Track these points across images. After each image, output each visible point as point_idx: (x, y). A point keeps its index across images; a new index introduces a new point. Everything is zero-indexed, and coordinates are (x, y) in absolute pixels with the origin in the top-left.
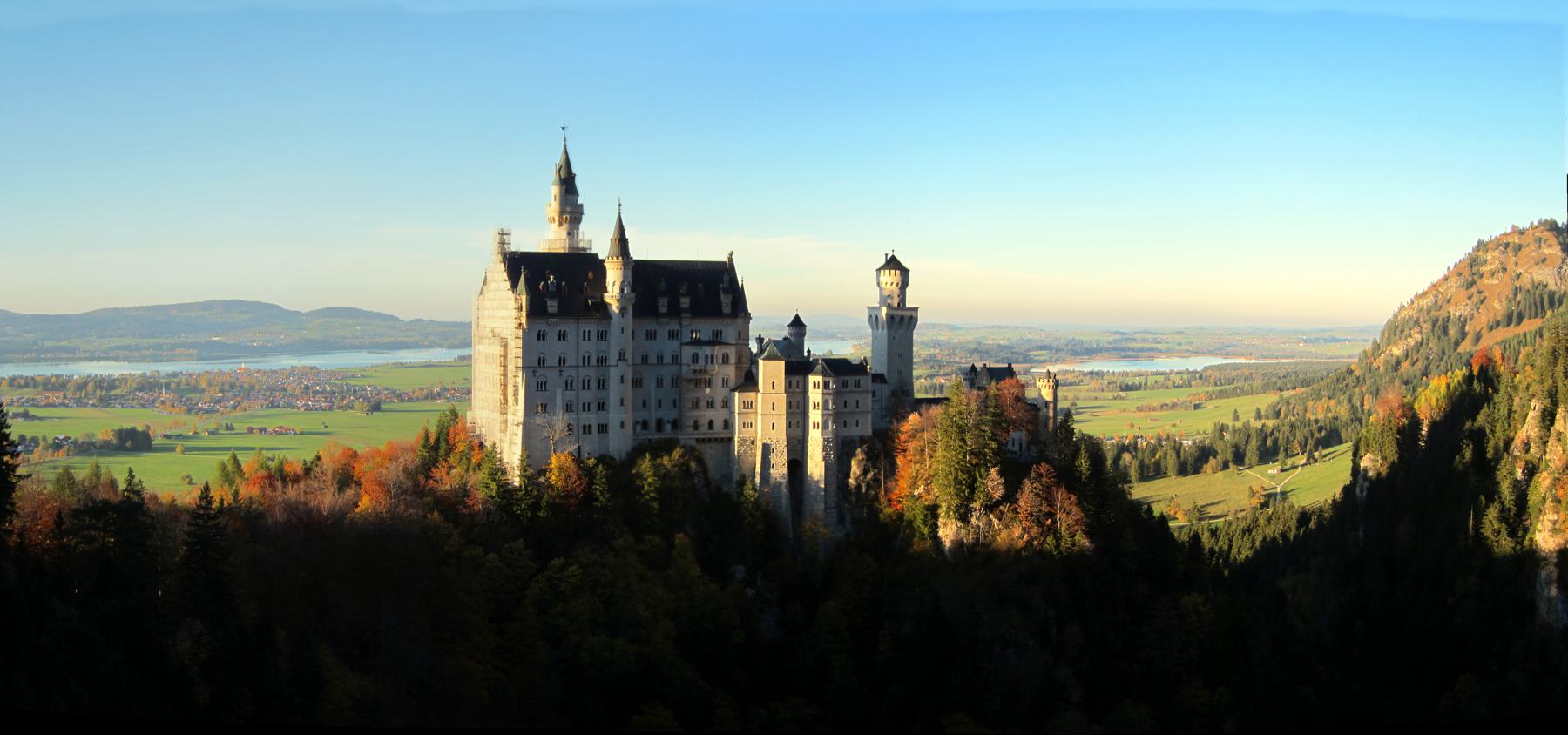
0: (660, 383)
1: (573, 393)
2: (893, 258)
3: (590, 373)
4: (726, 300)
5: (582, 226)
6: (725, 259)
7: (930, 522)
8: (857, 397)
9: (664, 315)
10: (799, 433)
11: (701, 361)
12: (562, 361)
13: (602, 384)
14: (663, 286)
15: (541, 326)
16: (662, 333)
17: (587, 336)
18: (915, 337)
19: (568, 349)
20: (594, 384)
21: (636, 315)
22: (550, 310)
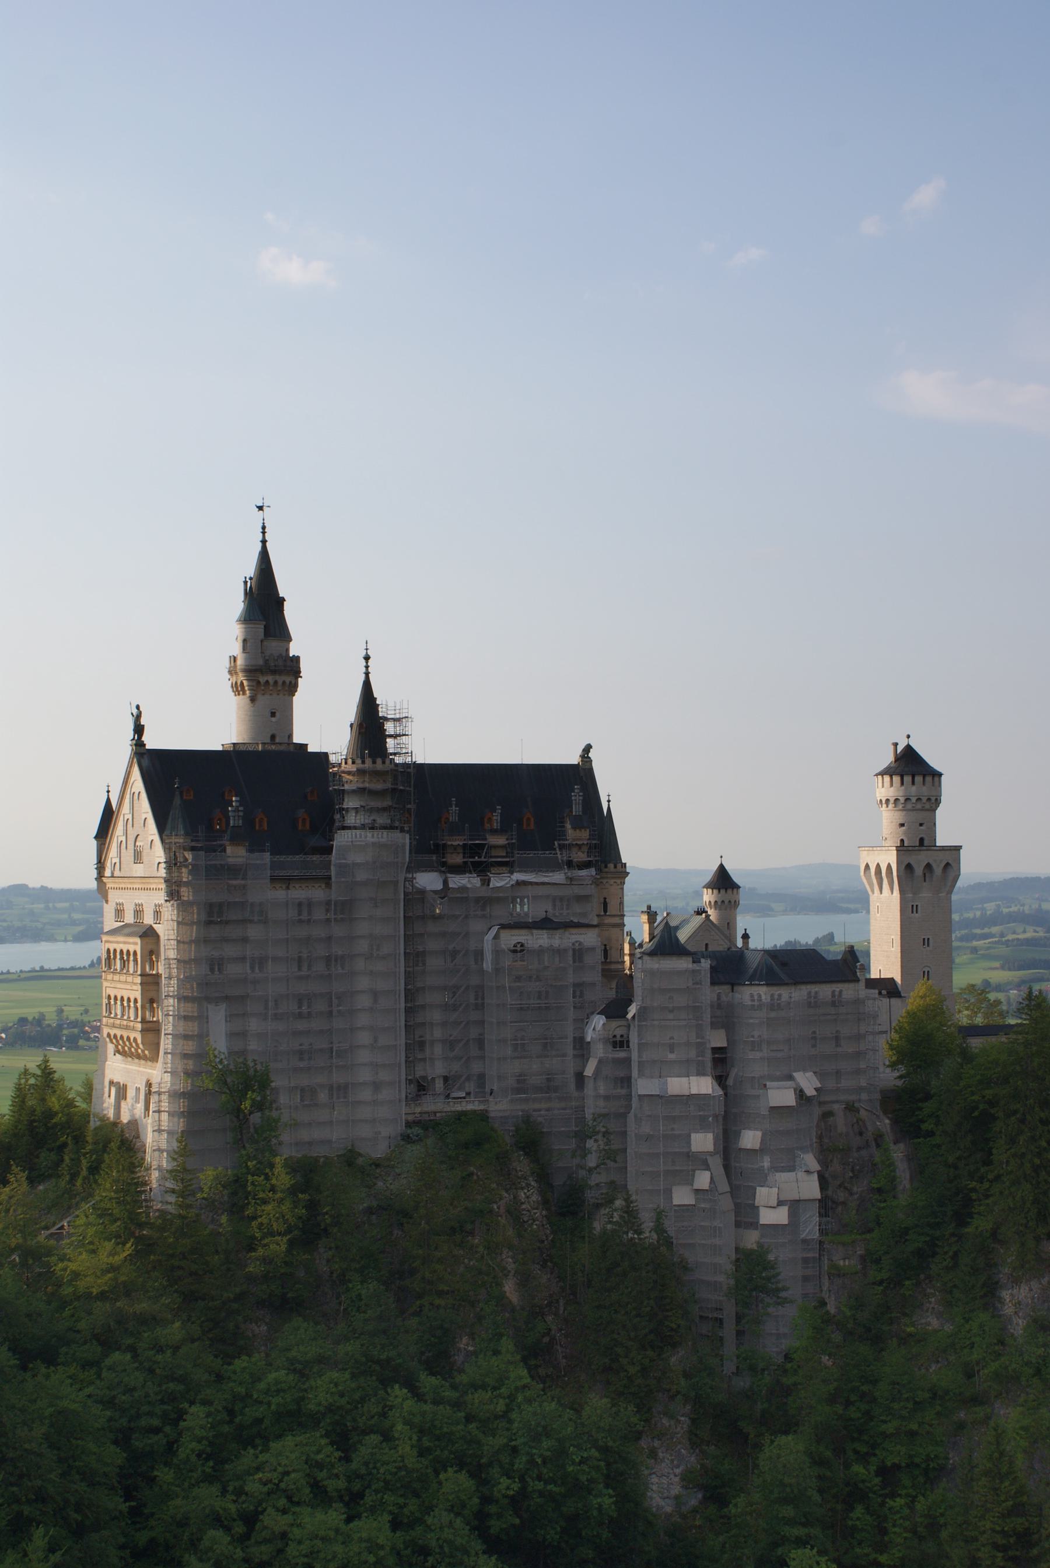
5: (297, 699)
6: (574, 759)
14: (453, 812)
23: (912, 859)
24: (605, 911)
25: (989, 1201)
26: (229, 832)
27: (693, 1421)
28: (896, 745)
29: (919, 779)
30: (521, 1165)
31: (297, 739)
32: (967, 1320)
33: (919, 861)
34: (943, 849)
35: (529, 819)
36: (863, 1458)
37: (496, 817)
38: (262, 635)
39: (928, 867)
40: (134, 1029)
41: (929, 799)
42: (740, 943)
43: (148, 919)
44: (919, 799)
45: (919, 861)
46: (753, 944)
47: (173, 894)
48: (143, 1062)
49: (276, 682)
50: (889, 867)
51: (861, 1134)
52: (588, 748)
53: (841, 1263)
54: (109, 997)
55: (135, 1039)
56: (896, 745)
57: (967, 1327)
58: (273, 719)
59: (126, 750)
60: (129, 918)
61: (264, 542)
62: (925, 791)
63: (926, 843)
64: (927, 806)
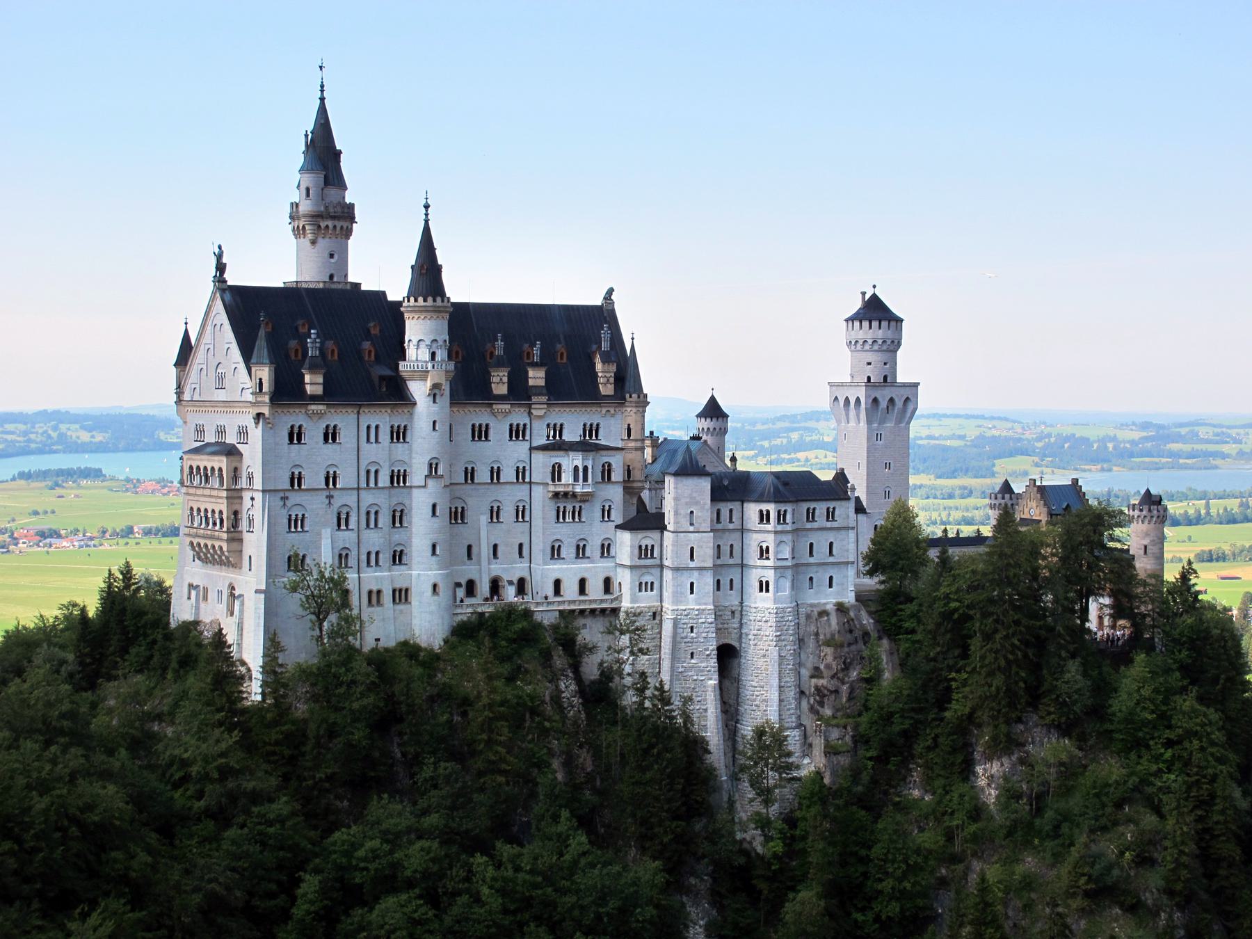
0: (495, 514)
1: (352, 536)
3: (381, 500)
4: (604, 372)
6: (597, 301)
7: (960, 758)
8: (831, 537)
9: (501, 398)
11: (567, 478)
12: (331, 479)
13: (399, 517)
15: (295, 417)
17: (372, 434)
18: (912, 435)
19: (341, 457)
20: (384, 520)
21: (455, 400)
22: (309, 389)
23: (877, 394)
24: (629, 435)
25: (967, 689)
26: (307, 361)
27: (715, 880)
28: (864, 294)
29: (884, 324)
30: (559, 660)
32: (947, 793)
33: (884, 395)
34: (904, 385)
35: (562, 354)
36: (863, 910)
37: (536, 351)
39: (892, 400)
40: (219, 539)
43: (231, 439)
45: (884, 395)
50: (858, 401)
51: (851, 631)
52: (610, 291)
54: (192, 509)
55: (221, 548)
56: (864, 294)
57: (948, 797)
60: (210, 438)
61: (322, 99)
62: (890, 334)
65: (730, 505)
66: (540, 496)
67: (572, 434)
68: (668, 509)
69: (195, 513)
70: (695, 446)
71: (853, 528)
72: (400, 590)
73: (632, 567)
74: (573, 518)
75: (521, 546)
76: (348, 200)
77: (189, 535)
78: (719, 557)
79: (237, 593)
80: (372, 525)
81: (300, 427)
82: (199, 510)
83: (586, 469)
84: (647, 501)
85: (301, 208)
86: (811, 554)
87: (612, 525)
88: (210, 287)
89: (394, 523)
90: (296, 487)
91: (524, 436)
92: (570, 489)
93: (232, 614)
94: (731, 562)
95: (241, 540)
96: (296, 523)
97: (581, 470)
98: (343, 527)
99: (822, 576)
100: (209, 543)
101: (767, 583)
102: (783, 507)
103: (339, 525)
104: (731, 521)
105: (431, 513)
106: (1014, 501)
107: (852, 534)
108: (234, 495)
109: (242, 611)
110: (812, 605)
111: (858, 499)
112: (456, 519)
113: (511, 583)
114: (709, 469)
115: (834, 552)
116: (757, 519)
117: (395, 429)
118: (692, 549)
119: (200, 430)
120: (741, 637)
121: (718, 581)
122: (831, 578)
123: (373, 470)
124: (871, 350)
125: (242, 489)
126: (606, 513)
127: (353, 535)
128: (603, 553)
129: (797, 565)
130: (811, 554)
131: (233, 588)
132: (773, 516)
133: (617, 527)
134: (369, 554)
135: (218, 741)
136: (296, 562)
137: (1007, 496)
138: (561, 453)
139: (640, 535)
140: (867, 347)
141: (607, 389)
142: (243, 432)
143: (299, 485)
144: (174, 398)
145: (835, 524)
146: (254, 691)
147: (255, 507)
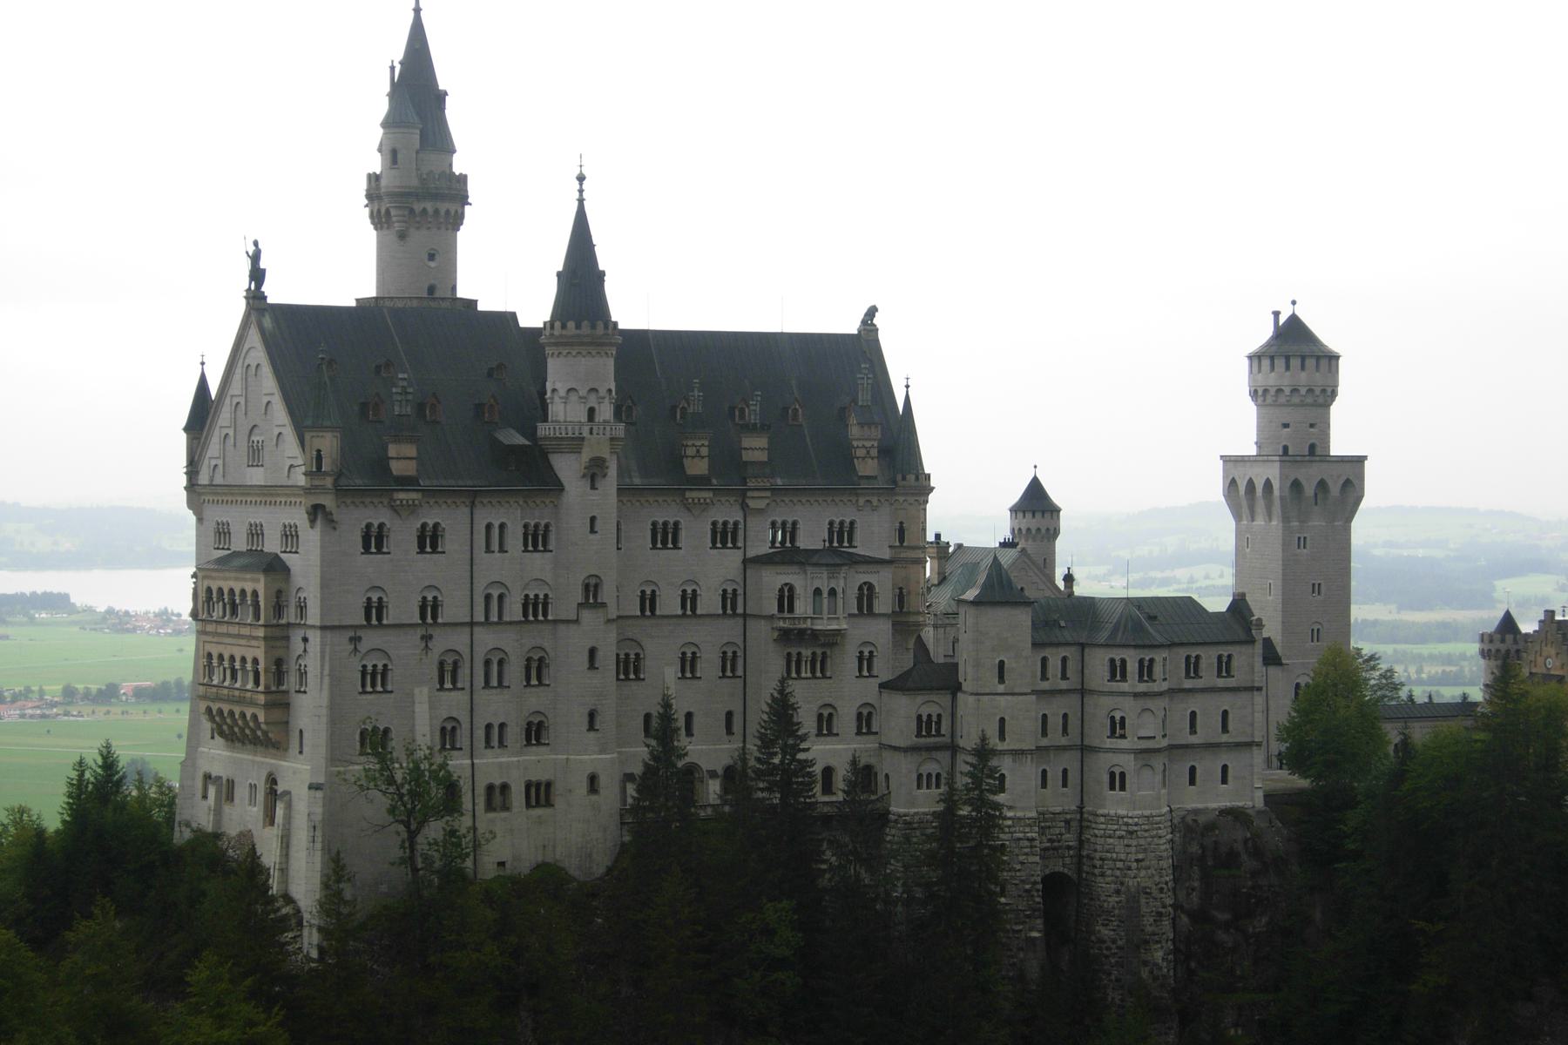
0: (689, 664)
1: (461, 698)
2: (1294, 320)
5: (463, 236)
6: (852, 327)
8: (1226, 701)
9: (701, 482)
10: (1061, 801)
11: (802, 607)
12: (430, 608)
13: (536, 669)
15: (378, 515)
16: (696, 531)
17: (495, 539)
19: (444, 574)
20: (515, 672)
22: (397, 468)
24: (902, 539)
28: (1276, 314)
31: (461, 293)
33: (1309, 476)
38: (418, 146)
39: (1322, 485)
40: (253, 703)
41: (1324, 391)
42: (1061, 584)
43: (272, 545)
44: (1310, 391)
46: (1079, 590)
47: (316, 512)
48: (260, 749)
49: (437, 212)
50: (1268, 485)
52: (872, 312)
53: (1232, 1032)
55: (255, 717)
56: (1276, 314)
58: (432, 264)
59: (237, 308)
60: (239, 543)
63: (1319, 451)
64: (1321, 400)
65: (1063, 652)
66: (762, 633)
67: (811, 537)
68: (964, 657)
69: (215, 662)
70: (1007, 557)
71: (1259, 689)
72: (538, 785)
73: (906, 750)
74: (813, 671)
75: (729, 715)
76: (457, 170)
77: (204, 698)
78: (1044, 733)
79: (280, 788)
80: (494, 682)
81: (381, 526)
82: (221, 657)
83: (833, 592)
84: (931, 648)
85: (383, 182)
86: (1193, 730)
87: (874, 683)
88: (240, 307)
89: (528, 678)
90: (374, 622)
91: (734, 541)
92: (808, 624)
93: (272, 823)
94: (1064, 741)
95: (286, 706)
96: (375, 678)
97: (825, 595)
98: (448, 685)
99: (1208, 767)
100: (237, 710)
101: (1123, 775)
102: (1147, 655)
103: (442, 681)
104: (1064, 677)
105: (586, 665)
106: (1521, 646)
107: (1259, 699)
108: (278, 635)
109: (288, 818)
110: (1196, 812)
111: (1268, 642)
112: (626, 673)
113: (713, 774)
114: (1030, 594)
115: (1230, 727)
116: (1107, 675)
117: (531, 528)
118: (1002, 720)
119: (223, 532)
120: (1080, 864)
121: (1044, 772)
122: (1225, 768)
123: (495, 593)
124: (1288, 404)
125: (289, 625)
126: (865, 661)
127: (461, 698)
128: (859, 728)
129: (1172, 747)
130: (1193, 730)
131: (274, 782)
132: (1133, 667)
133: (882, 686)
134: (489, 727)
135: (251, 1024)
136: (375, 740)
137: (1509, 637)
138: (795, 568)
139: (920, 699)
140: (1282, 400)
141: (868, 467)
142: (290, 535)
143: (379, 618)
144: (183, 481)
145: (1231, 682)
146: (310, 941)
147: (312, 654)
